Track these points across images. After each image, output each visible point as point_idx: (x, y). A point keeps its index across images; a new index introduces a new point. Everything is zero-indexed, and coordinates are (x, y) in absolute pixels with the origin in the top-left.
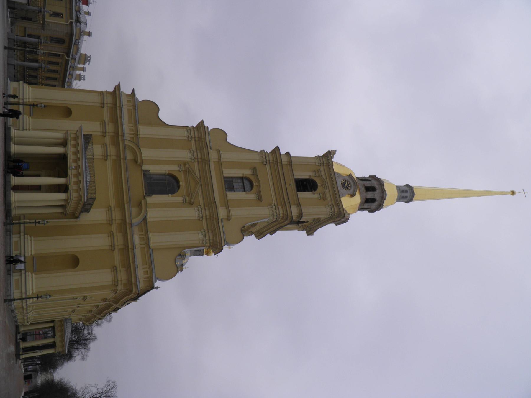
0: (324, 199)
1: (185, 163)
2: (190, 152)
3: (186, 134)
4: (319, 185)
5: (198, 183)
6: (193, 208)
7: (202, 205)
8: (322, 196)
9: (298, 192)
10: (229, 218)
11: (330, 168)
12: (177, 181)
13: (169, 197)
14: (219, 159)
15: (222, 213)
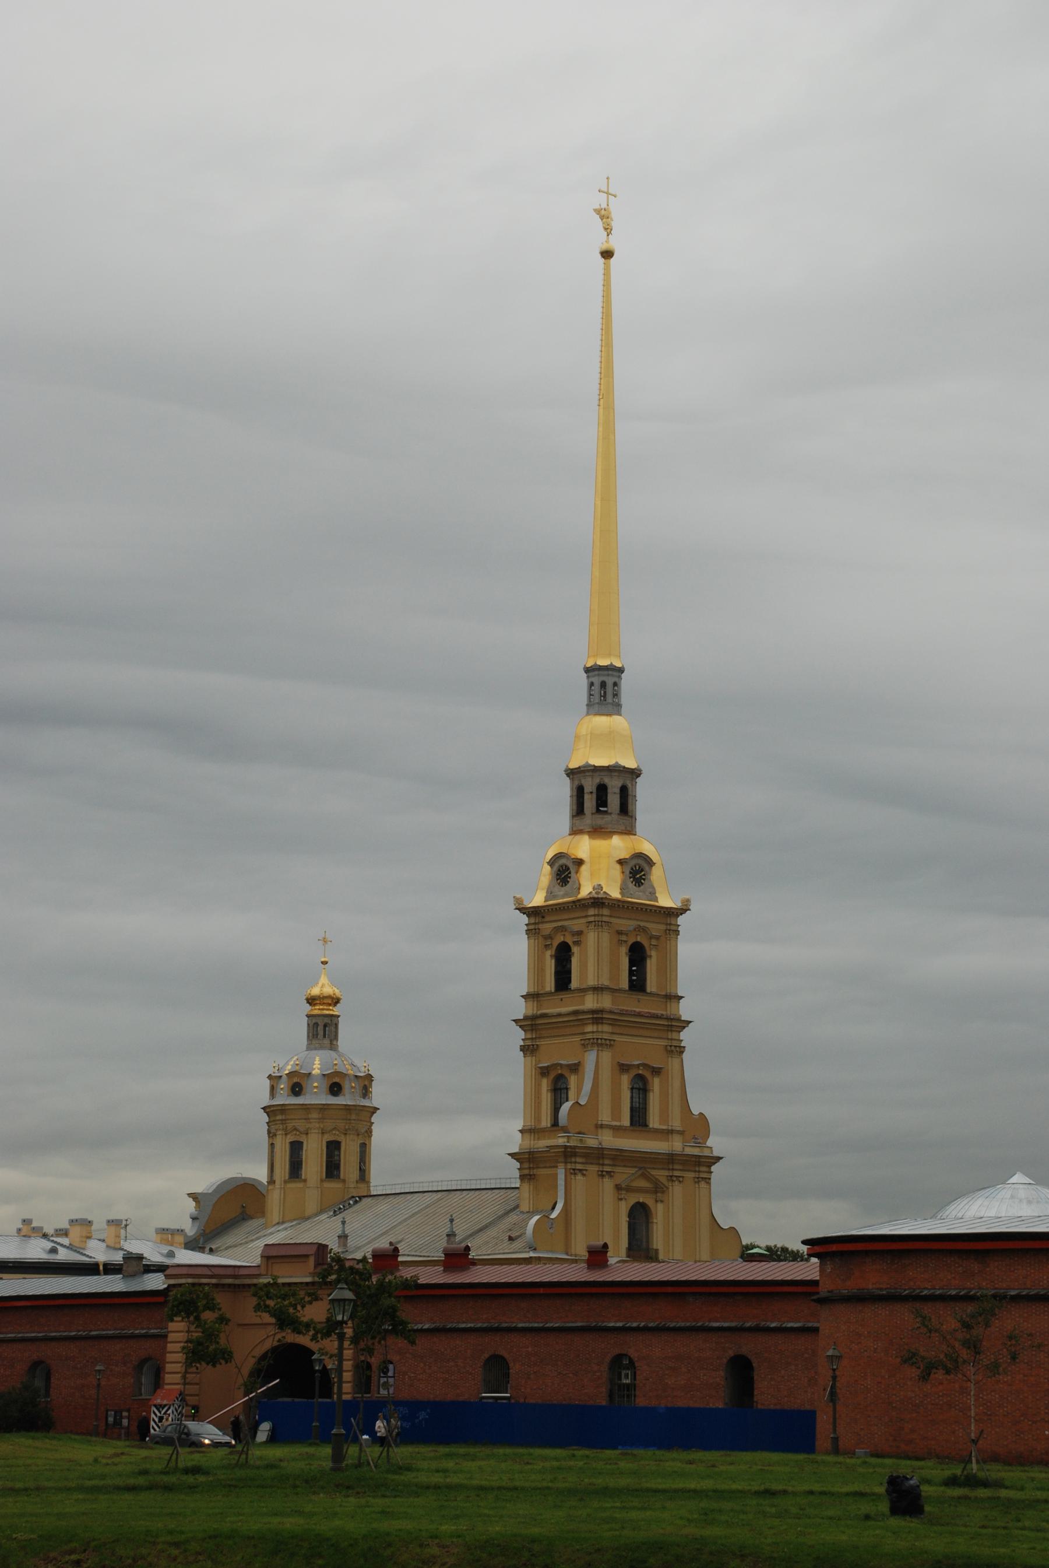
0: (657, 938)
1: (618, 1188)
2: (603, 1176)
3: (579, 1177)
4: (639, 939)
5: (643, 1172)
6: (671, 1187)
7: (666, 1173)
8: (654, 942)
9: (648, 990)
10: (681, 1133)
11: (619, 905)
12: (638, 1203)
13: (657, 1223)
14: (610, 1128)
15: (676, 1145)
